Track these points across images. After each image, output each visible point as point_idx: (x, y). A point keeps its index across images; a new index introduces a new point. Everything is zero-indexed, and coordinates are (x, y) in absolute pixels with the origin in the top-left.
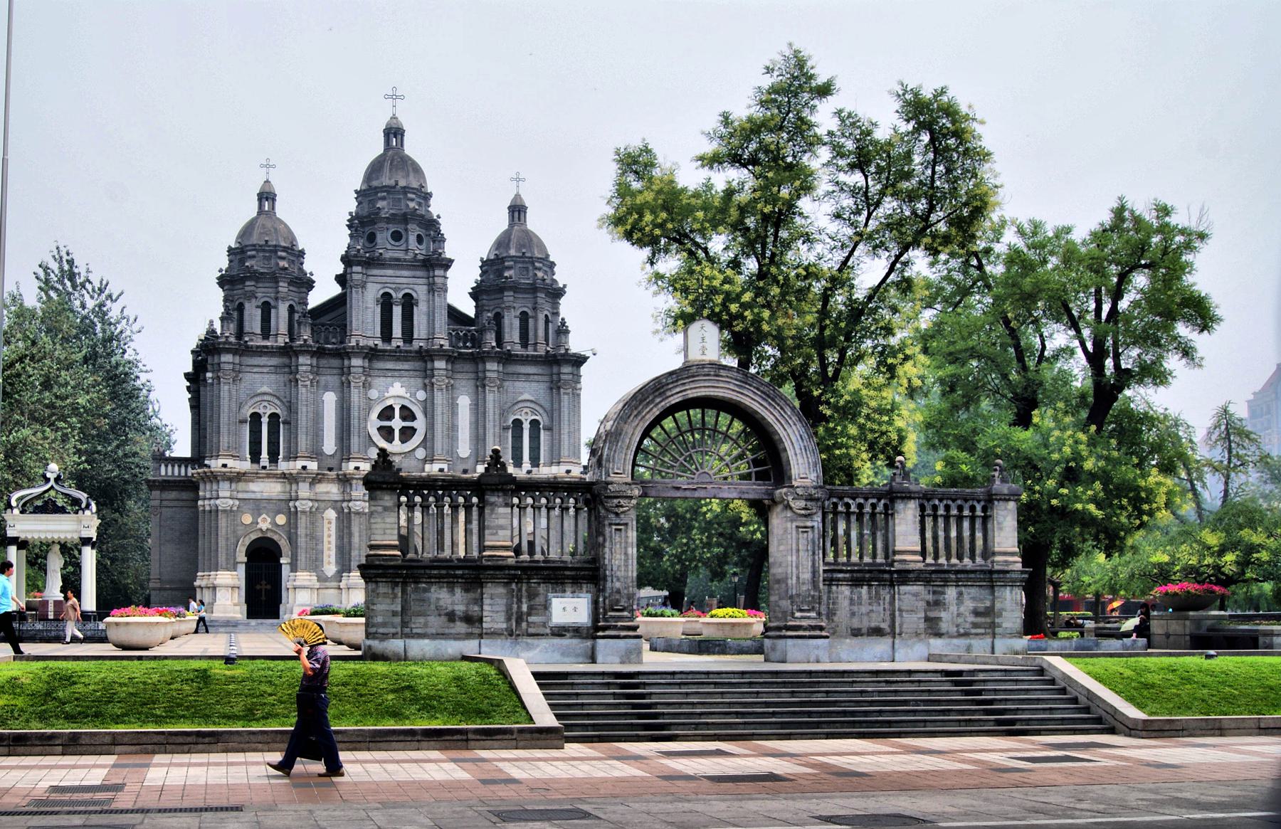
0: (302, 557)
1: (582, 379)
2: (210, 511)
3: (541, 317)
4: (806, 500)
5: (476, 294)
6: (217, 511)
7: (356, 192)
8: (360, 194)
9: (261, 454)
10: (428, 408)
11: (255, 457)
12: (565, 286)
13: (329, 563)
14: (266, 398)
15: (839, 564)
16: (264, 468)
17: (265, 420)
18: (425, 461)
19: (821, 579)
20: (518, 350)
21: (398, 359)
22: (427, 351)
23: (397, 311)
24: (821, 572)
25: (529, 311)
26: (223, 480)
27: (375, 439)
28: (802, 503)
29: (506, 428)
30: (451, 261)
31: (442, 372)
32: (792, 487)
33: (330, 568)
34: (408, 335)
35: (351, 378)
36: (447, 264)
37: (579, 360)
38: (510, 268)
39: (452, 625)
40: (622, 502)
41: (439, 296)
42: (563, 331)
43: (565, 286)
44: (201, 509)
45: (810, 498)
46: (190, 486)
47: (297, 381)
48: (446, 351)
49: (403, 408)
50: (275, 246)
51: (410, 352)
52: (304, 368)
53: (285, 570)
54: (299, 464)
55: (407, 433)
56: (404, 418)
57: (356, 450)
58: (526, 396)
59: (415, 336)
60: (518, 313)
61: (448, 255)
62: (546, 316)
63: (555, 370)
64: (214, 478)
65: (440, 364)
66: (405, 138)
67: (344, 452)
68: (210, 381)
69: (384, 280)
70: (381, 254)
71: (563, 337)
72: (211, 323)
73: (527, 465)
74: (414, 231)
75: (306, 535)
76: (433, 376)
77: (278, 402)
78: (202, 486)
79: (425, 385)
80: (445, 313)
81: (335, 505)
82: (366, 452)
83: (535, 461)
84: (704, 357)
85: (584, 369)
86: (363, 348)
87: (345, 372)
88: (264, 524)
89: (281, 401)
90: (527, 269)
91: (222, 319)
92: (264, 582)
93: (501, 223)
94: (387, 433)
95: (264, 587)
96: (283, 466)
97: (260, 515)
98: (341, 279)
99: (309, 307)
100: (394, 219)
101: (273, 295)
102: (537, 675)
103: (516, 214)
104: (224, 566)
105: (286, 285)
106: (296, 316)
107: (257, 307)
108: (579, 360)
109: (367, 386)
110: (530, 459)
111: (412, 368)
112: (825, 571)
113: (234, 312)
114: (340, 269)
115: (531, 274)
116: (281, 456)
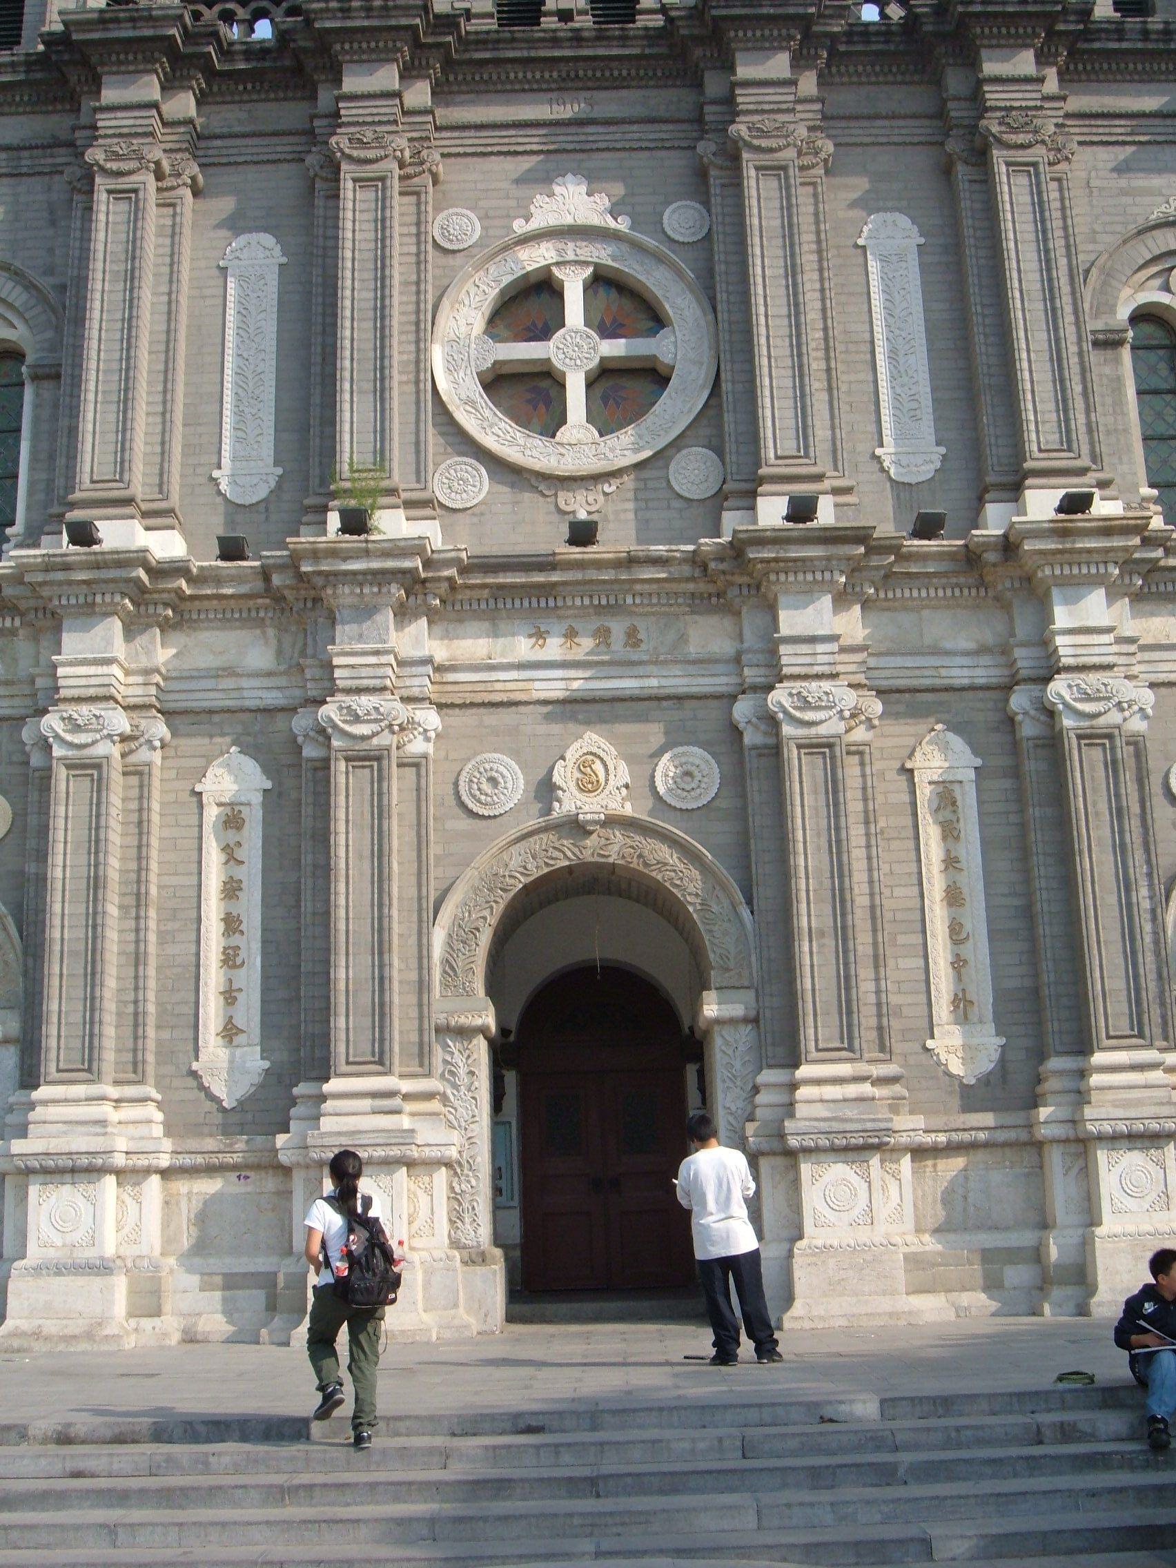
18: (719, 500)
27: (467, 420)
29: (1108, 342)
35: (339, 141)
52: (124, 121)
79: (701, 174)
82: (420, 472)
89: (30, 286)
111: (639, 111)
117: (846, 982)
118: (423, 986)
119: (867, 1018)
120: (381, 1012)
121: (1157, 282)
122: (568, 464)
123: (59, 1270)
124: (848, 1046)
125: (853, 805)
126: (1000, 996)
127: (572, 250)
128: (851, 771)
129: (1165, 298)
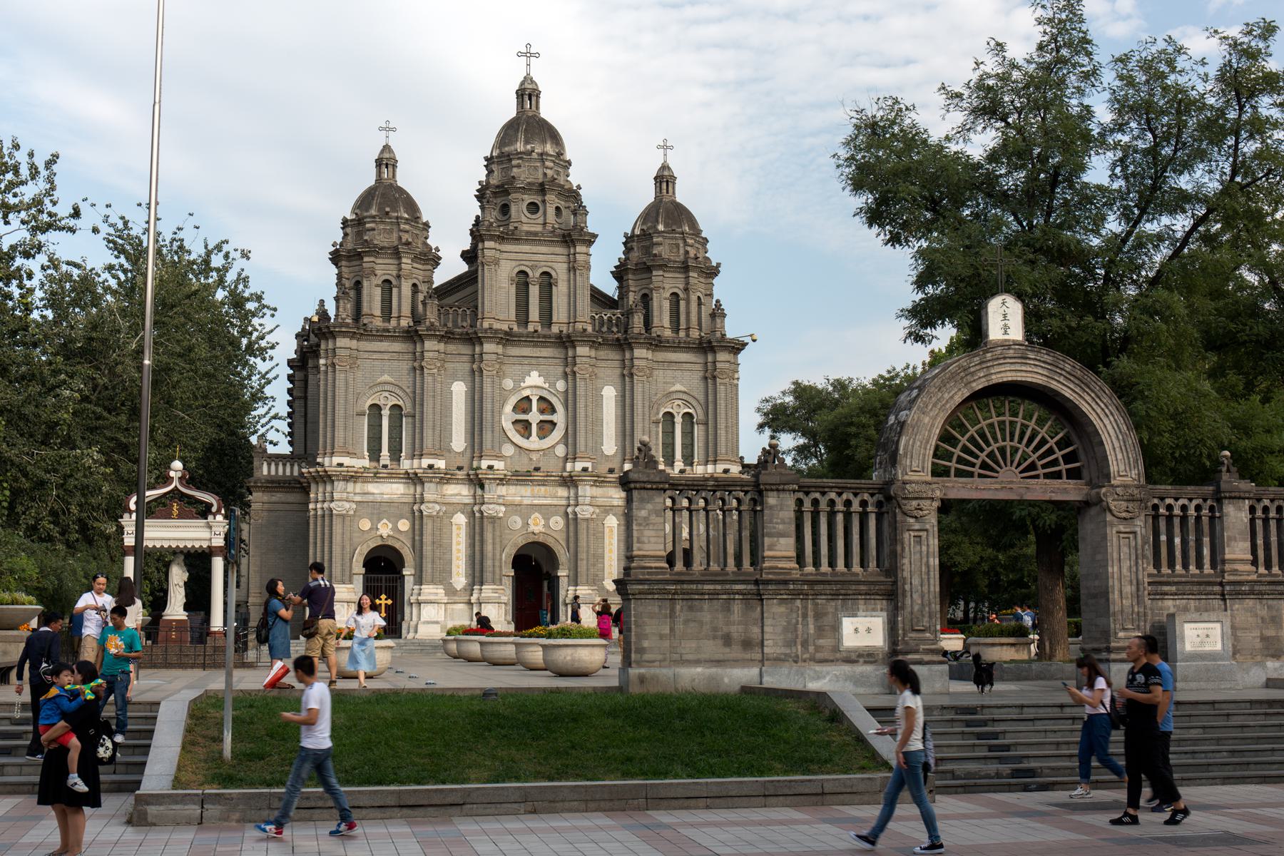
0: (428, 567)
1: (740, 368)
3: (694, 298)
4: (1128, 501)
5: (620, 274)
6: (331, 515)
7: (486, 159)
8: (489, 160)
10: (570, 399)
11: (375, 454)
12: (719, 265)
13: (458, 574)
14: (387, 387)
15: (1163, 576)
16: (385, 466)
17: (386, 413)
18: (566, 459)
19: (1146, 592)
20: (668, 333)
21: (536, 344)
22: (569, 336)
23: (534, 291)
24: (1146, 585)
26: (338, 480)
27: (510, 434)
28: (1124, 504)
29: (657, 422)
30: (595, 236)
31: (584, 359)
32: (1112, 486)
33: (460, 579)
34: (547, 317)
35: (483, 366)
36: (590, 239)
37: (737, 347)
38: (659, 244)
39: (727, 650)
40: (922, 503)
41: (581, 275)
42: (718, 313)
43: (719, 265)
44: (312, 513)
45: (1131, 499)
46: (301, 487)
47: (422, 368)
49: (541, 399)
50: (397, 218)
51: (550, 337)
52: (431, 354)
53: (409, 582)
54: (425, 462)
55: (546, 427)
56: (542, 412)
57: (489, 446)
59: (555, 319)
60: (668, 295)
61: (590, 230)
62: (699, 298)
64: (327, 478)
65: (582, 350)
66: (541, 100)
68: (323, 368)
69: (521, 256)
70: (516, 228)
71: (718, 320)
72: (322, 302)
73: (679, 465)
74: (553, 200)
75: (433, 543)
77: (401, 393)
78: (313, 487)
80: (588, 293)
81: (462, 508)
83: (689, 459)
84: (1006, 337)
85: (742, 357)
86: (497, 331)
87: (476, 359)
88: (385, 529)
90: (678, 246)
91: (337, 299)
92: (383, 597)
93: (647, 195)
94: (524, 427)
95: (383, 602)
96: (406, 464)
97: (379, 520)
98: (470, 256)
99: (434, 286)
100: (530, 190)
101: (394, 273)
102: (870, 710)
103: (664, 185)
104: (339, 578)
105: (409, 261)
106: (421, 297)
107: (377, 286)
108: (737, 347)
109: (500, 375)
110: (683, 456)
112: (1150, 584)
113: (350, 290)
114: (467, 245)
115: (682, 251)
116: (403, 454)
117: (588, 570)
118: (501, 567)
119: (591, 577)
120: (494, 572)
122: (532, 447)
123: (428, 622)
124: (587, 583)
125: (591, 532)
127: (535, 391)
128: (592, 525)
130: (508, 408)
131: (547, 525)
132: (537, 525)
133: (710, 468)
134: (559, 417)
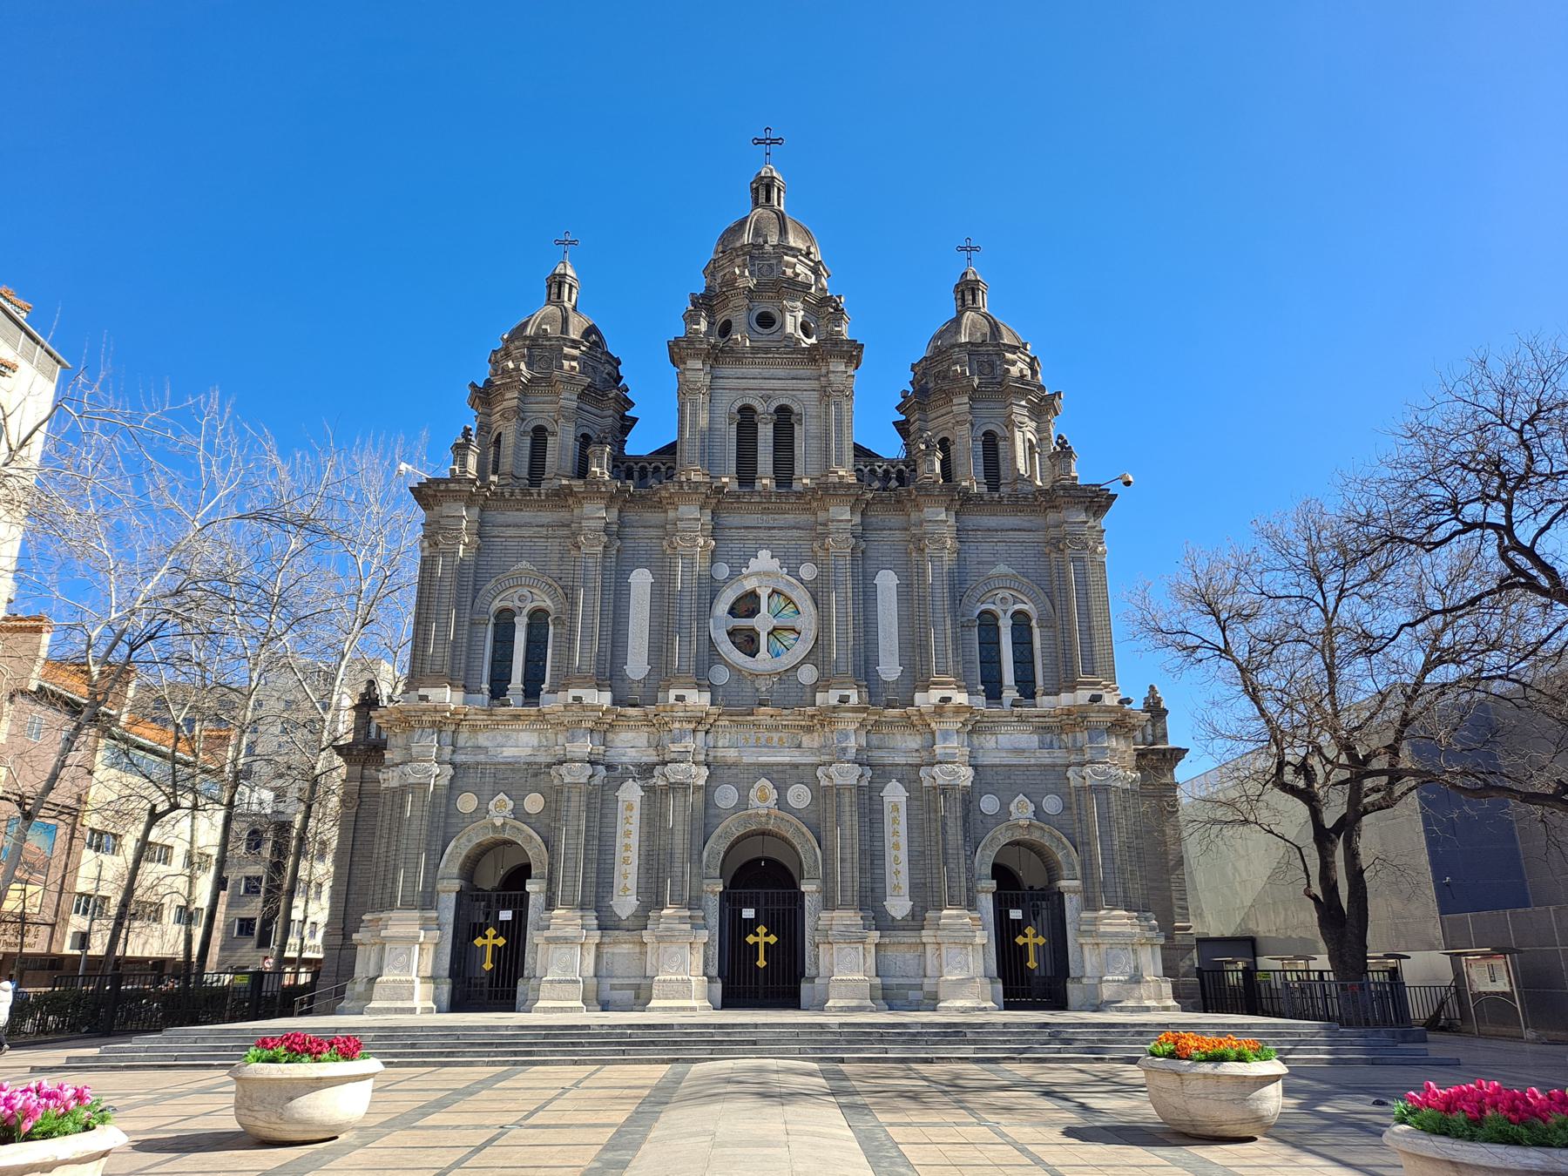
2: (393, 791)
9: (510, 683)
13: (626, 889)
18: (815, 688)
23: (766, 433)
25: (998, 431)
37: (1098, 501)
48: (850, 486)
54: (573, 692)
58: (1002, 568)
63: (1052, 517)
67: (662, 674)
69: (744, 383)
73: (1010, 694)
76: (825, 535)
85: (1105, 521)
88: (500, 810)
95: (490, 942)
107: (524, 433)
108: (1098, 501)
121: (991, 600)
126: (912, 887)
129: (993, 607)
130: (722, 607)
131: (781, 803)
132: (762, 797)
133: (1065, 699)
134: (807, 621)
